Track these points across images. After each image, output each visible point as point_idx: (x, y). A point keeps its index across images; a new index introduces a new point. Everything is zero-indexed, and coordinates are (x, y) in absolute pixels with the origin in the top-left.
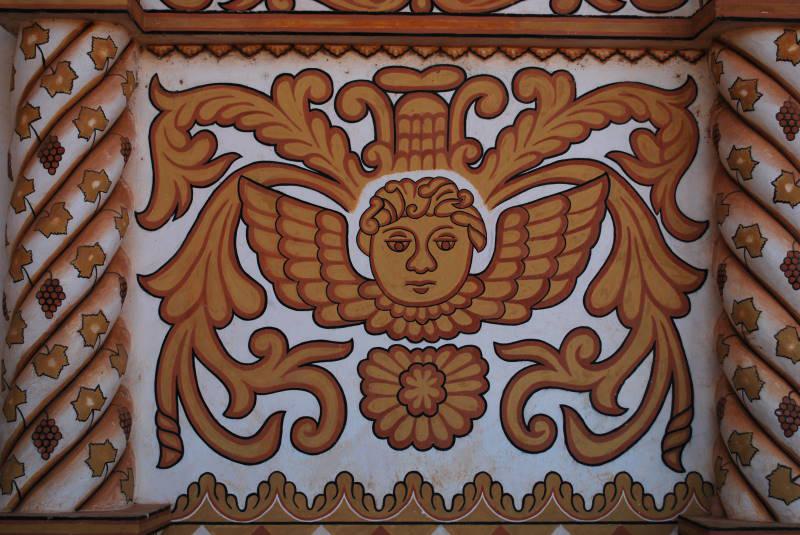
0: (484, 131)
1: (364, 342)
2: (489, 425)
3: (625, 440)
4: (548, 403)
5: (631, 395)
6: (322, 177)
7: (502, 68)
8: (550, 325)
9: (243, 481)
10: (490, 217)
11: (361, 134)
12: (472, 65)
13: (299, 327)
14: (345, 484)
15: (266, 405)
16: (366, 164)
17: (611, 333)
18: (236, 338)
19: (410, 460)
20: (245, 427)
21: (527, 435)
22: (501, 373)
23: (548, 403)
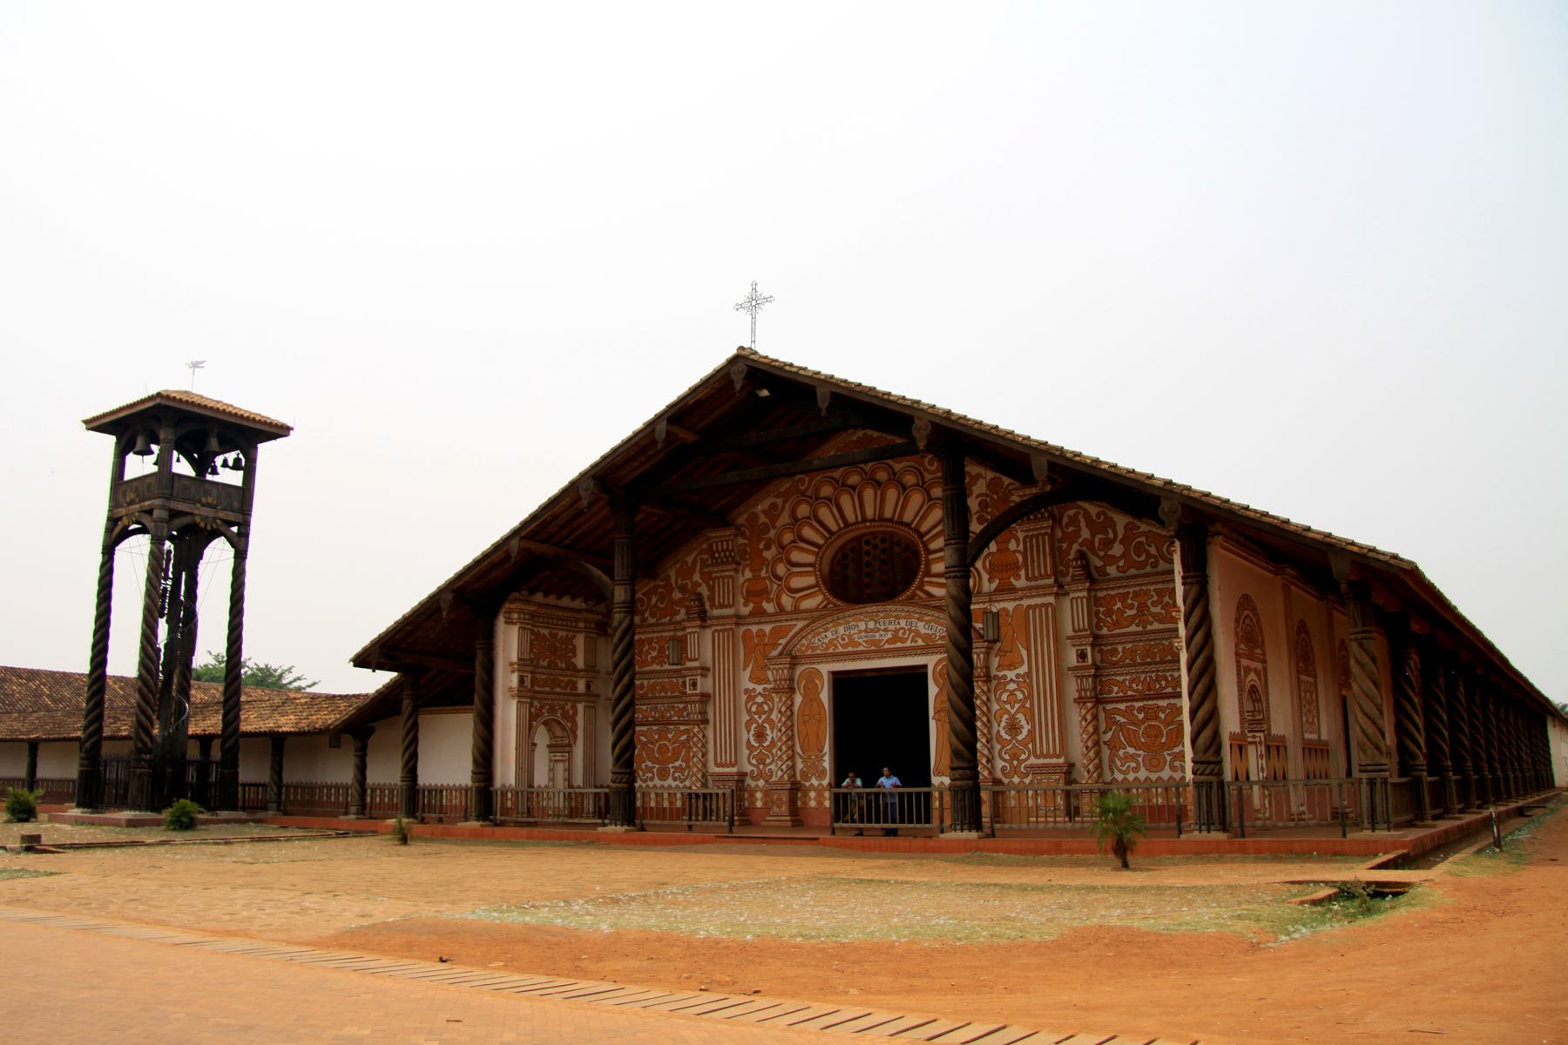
0: (670, 736)
1: (657, 766)
2: (670, 778)
3: (685, 779)
4: (676, 775)
5: (686, 774)
6: (652, 743)
7: (672, 727)
8: (677, 764)
9: (644, 785)
10: (670, 749)
11: (656, 737)
12: (669, 727)
13: (650, 764)
14: (655, 786)
15: (647, 775)
16: (657, 741)
17: (684, 765)
18: (643, 766)
19: (662, 783)
20: (644, 778)
21: (675, 779)
22: (672, 770)
23: (676, 775)
